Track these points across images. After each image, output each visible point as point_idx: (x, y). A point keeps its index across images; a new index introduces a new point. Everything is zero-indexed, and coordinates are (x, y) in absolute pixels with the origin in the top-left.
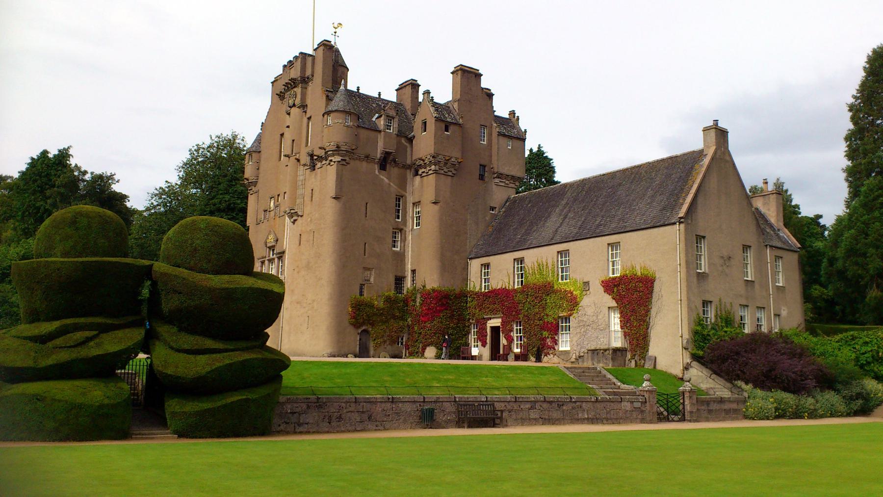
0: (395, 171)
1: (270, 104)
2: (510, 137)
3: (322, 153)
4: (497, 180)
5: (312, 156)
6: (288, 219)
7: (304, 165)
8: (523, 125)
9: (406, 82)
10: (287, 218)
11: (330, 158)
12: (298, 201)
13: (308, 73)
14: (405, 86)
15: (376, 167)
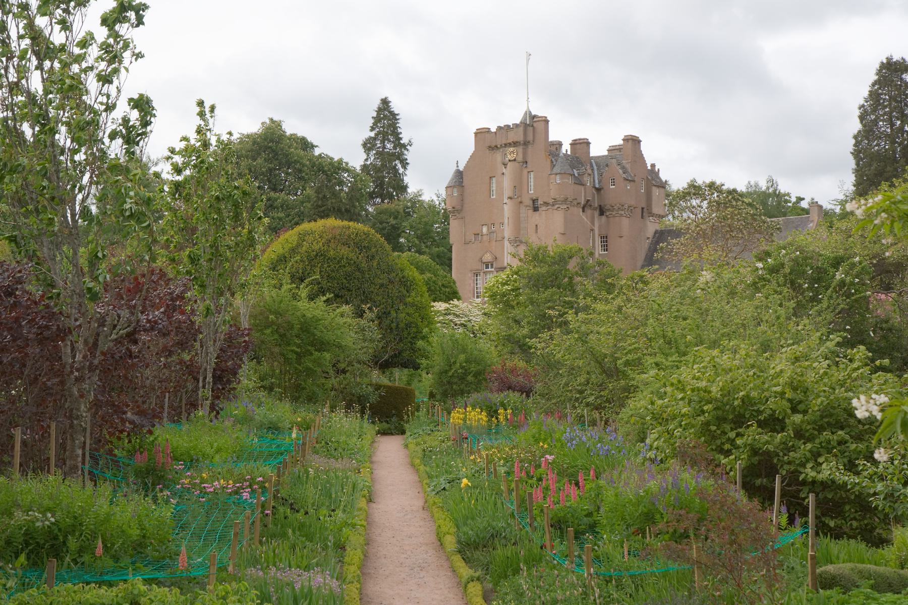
0: (589, 211)
1: (473, 149)
2: (658, 186)
3: (551, 201)
4: (651, 218)
5: (535, 201)
6: (509, 245)
7: (527, 206)
8: (663, 176)
9: (580, 139)
10: (506, 243)
11: (557, 206)
12: (522, 232)
13: (530, 138)
14: (580, 143)
15: (581, 210)
